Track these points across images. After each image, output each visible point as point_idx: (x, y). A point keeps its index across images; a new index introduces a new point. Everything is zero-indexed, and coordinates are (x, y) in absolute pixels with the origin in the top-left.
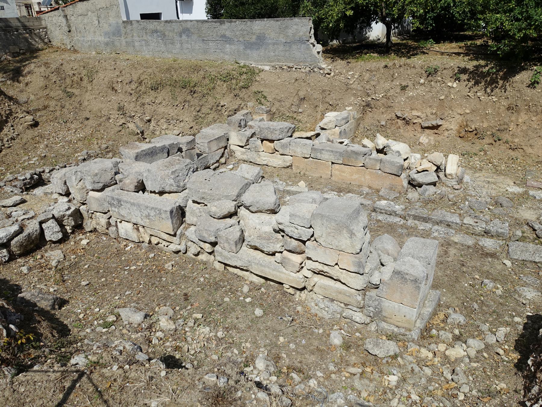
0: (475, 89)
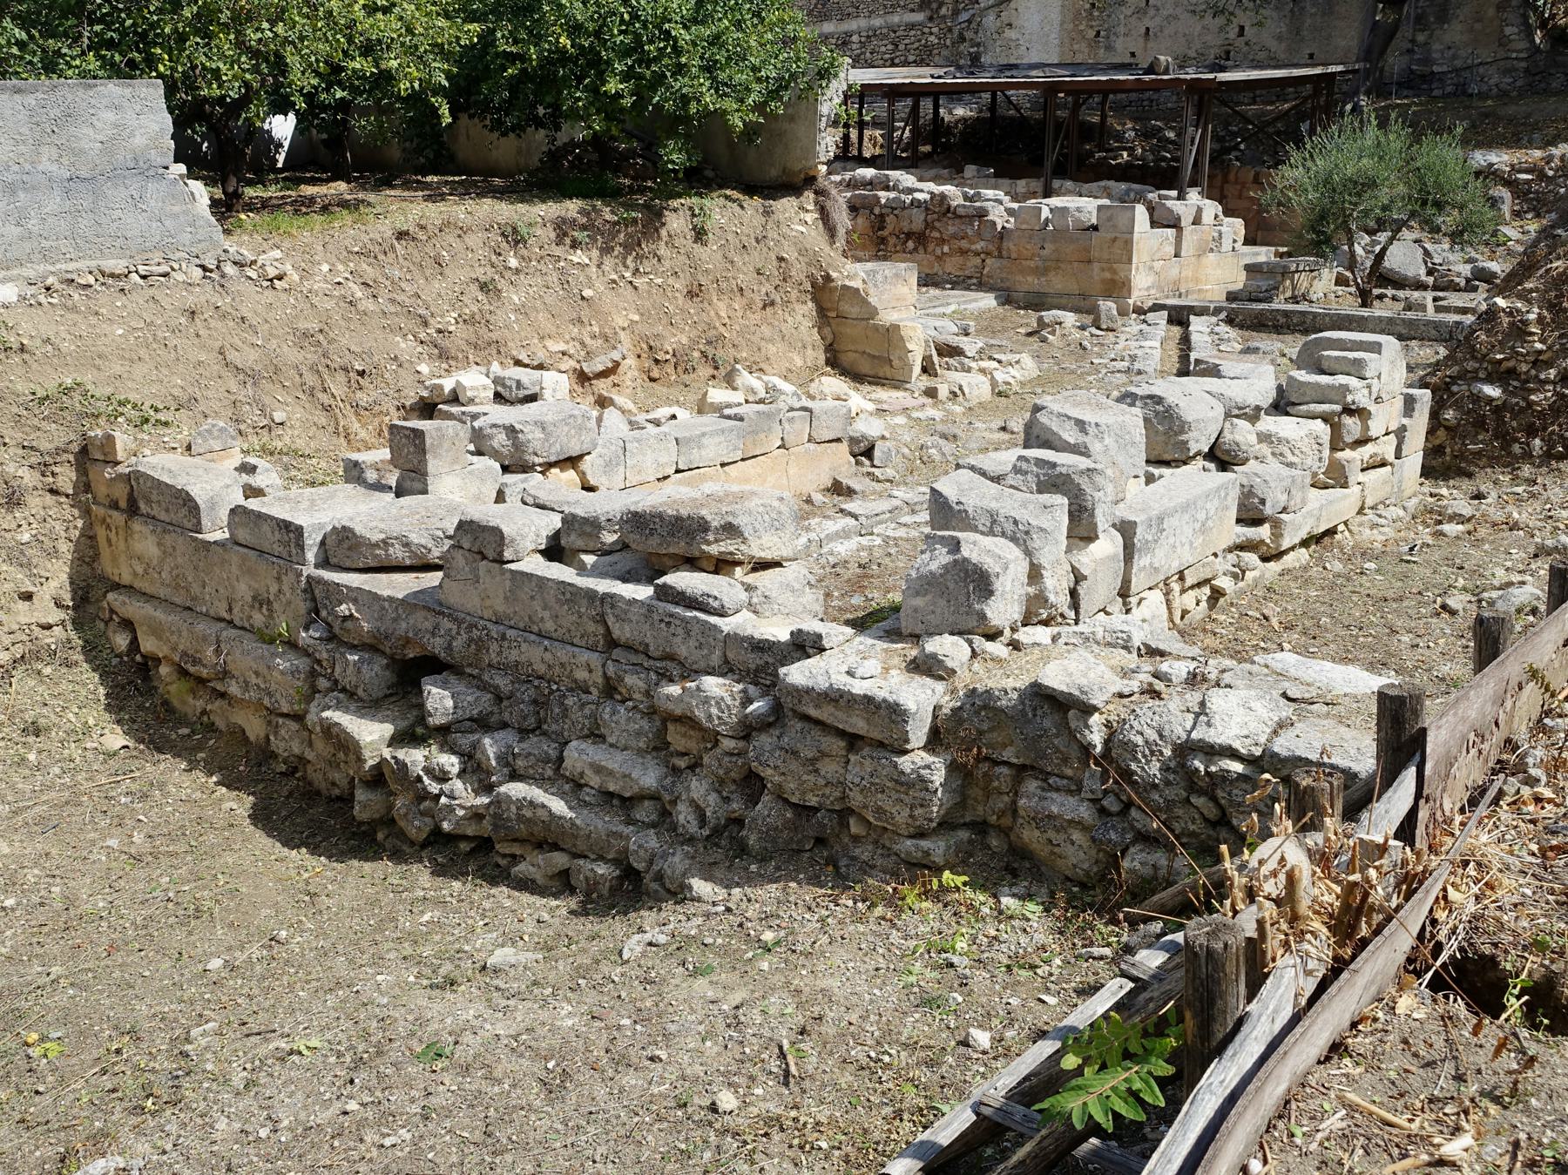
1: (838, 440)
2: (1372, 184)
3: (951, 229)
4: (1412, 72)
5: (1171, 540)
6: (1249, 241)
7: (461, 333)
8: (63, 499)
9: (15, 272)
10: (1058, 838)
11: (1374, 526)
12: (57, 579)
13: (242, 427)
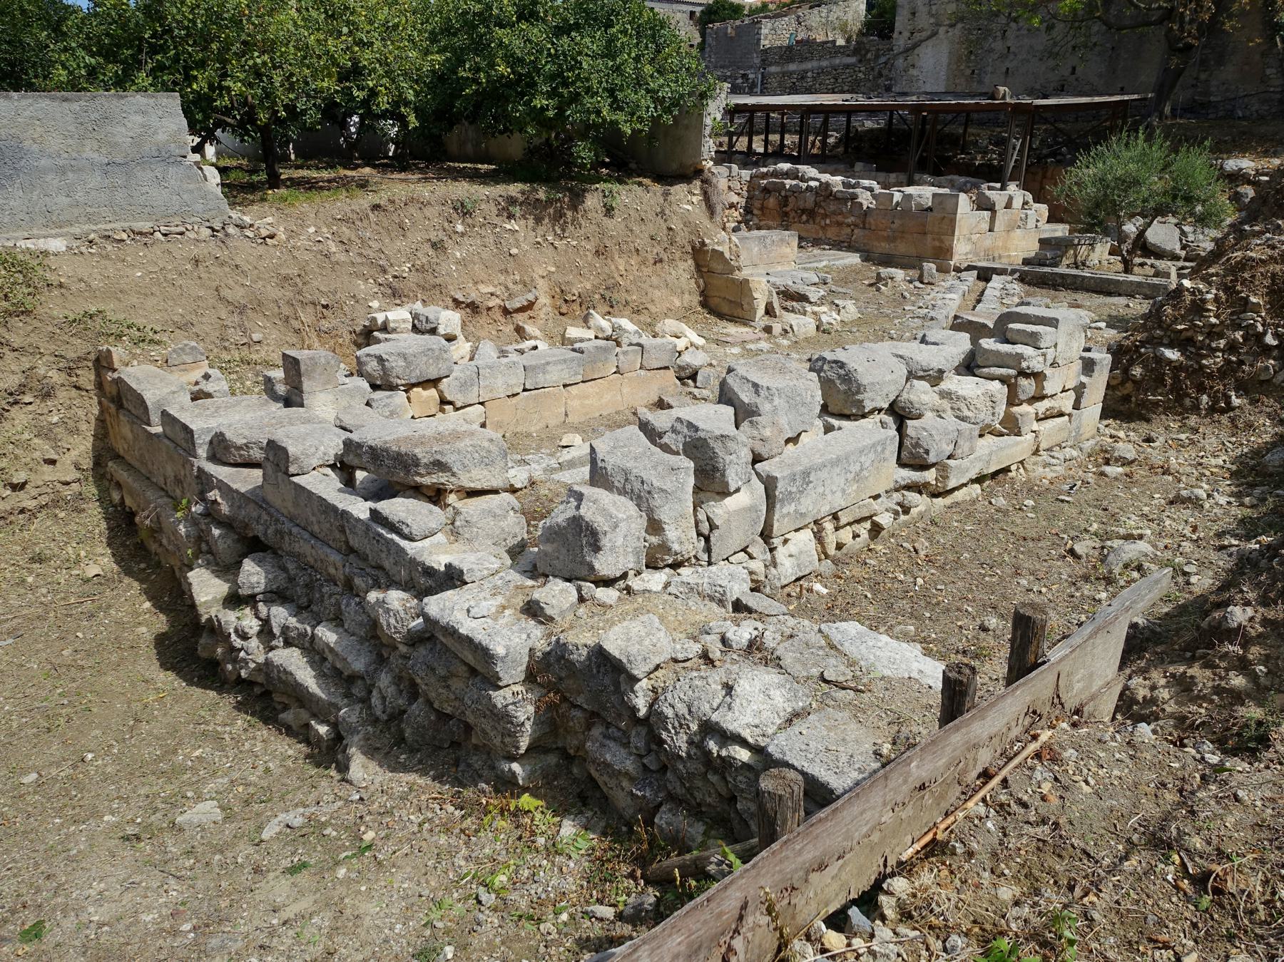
0: (541, 230)
1: (666, 368)
2: (1137, 182)
3: (832, 208)
4: (1195, 101)
5: (821, 490)
6: (1051, 220)
7: (414, 278)
8: (84, 393)
9: (65, 230)
10: (612, 783)
11: (1046, 465)
12: (81, 447)
13: (227, 344)
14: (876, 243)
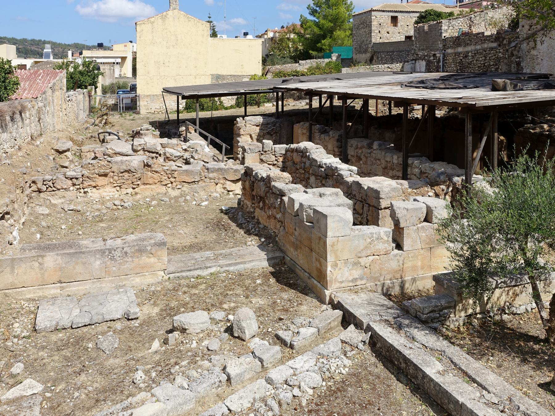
14: (288, 247)
